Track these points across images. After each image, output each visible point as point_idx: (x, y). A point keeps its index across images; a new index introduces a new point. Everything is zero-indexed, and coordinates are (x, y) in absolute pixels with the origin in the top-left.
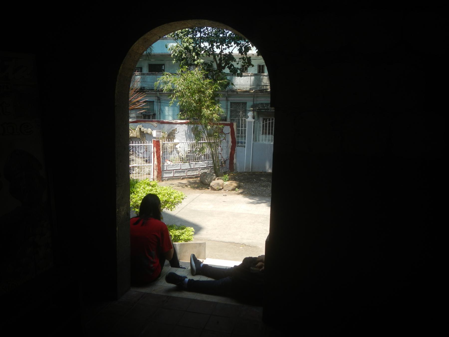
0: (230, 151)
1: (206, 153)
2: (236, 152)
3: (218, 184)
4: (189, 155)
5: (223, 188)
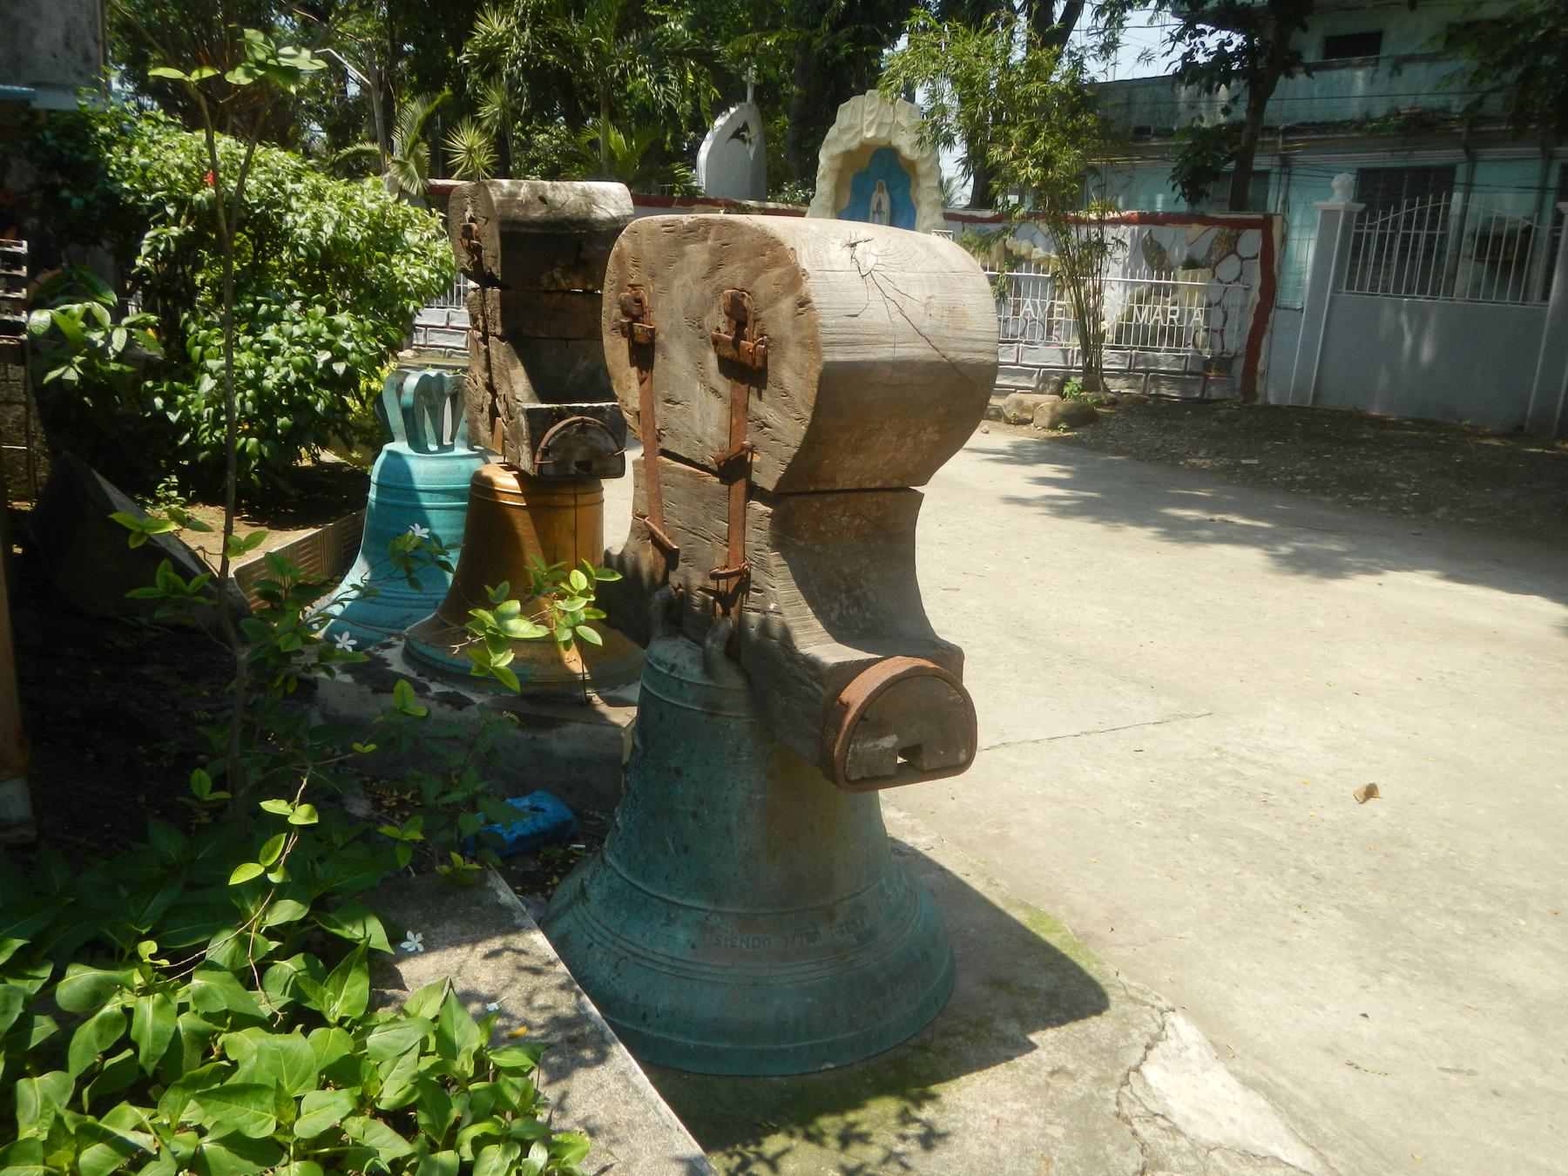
0: (1250, 322)
2: (1272, 331)
3: (1019, 404)
4: (1058, 322)
5: (1032, 421)
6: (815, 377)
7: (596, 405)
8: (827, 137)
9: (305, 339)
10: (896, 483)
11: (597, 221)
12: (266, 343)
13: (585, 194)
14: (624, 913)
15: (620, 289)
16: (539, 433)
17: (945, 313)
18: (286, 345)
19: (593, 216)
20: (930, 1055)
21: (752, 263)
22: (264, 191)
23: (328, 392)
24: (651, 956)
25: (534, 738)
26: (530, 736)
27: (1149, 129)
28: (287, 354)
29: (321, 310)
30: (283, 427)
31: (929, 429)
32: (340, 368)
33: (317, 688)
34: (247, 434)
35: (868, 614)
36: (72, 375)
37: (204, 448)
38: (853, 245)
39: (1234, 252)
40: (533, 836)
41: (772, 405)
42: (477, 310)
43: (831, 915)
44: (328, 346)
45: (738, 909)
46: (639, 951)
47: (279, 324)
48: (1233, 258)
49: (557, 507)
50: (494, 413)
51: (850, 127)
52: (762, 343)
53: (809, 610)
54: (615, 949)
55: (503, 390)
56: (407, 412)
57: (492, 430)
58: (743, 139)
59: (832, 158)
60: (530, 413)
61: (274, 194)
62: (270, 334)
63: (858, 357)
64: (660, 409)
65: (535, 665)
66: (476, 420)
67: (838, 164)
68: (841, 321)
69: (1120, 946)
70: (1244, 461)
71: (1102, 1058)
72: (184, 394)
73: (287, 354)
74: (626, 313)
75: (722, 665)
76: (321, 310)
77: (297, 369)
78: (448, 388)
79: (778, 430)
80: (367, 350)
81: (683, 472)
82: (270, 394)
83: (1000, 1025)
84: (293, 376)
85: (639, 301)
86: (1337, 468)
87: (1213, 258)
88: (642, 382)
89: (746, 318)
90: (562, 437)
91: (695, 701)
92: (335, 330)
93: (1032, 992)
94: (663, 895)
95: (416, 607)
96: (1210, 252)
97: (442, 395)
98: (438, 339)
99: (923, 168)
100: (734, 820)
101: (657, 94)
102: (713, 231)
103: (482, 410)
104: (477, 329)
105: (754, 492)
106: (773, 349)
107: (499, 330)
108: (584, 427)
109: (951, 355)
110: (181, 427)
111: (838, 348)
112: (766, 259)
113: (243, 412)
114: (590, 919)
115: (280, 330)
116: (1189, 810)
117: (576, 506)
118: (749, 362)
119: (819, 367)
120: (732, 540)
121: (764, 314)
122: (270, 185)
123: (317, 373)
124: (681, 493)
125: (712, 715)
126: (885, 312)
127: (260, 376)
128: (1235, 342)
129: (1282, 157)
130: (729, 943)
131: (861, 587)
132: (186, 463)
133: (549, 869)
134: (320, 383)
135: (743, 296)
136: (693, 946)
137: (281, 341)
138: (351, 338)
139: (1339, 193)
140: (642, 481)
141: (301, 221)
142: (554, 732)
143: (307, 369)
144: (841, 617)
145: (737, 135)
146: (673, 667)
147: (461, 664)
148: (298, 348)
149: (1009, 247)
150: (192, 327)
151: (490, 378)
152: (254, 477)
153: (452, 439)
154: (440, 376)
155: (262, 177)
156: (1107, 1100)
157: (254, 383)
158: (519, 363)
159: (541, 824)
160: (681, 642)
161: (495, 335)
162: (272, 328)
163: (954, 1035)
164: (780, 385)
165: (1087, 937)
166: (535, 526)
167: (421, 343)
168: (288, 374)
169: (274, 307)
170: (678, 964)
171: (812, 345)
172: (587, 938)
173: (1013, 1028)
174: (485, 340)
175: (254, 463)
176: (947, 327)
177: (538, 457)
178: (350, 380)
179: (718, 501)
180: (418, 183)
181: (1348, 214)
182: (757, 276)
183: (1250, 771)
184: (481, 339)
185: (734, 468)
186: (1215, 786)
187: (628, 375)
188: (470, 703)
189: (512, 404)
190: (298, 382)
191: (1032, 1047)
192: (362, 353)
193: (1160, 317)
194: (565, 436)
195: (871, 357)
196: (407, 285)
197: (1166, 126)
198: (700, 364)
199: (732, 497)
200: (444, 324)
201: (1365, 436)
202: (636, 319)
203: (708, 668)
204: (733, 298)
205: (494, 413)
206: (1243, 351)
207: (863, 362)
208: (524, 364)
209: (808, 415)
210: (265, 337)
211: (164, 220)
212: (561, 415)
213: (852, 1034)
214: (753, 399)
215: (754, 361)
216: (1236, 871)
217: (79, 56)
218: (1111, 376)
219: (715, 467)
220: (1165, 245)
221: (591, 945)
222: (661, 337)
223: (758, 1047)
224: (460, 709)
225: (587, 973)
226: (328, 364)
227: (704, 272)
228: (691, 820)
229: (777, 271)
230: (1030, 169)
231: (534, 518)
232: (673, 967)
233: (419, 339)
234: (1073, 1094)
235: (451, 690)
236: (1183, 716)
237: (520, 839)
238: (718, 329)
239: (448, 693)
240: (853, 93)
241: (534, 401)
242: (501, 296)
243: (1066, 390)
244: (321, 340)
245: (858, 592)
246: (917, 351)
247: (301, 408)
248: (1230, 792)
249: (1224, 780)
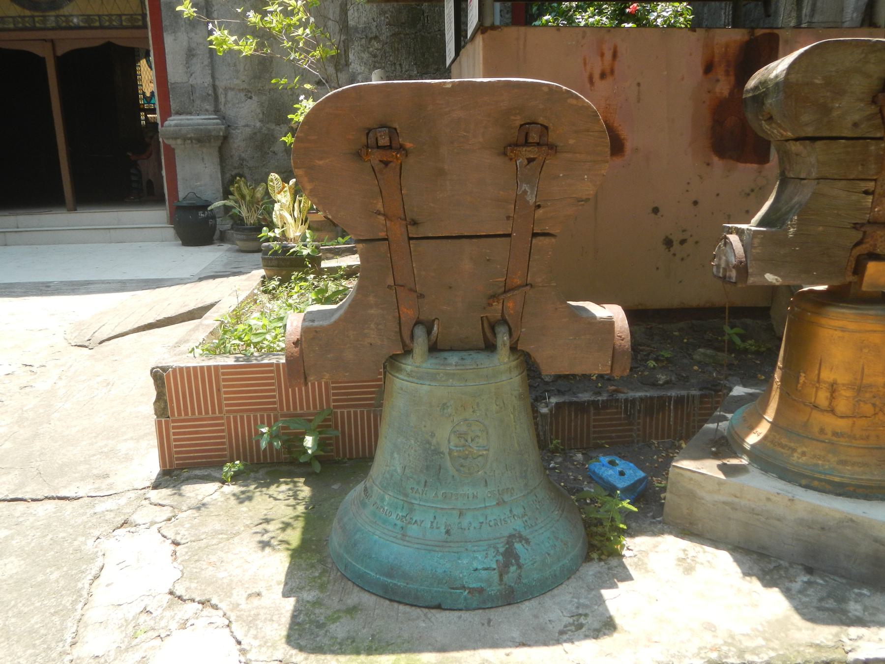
20: (316, 561)
71: (249, 616)
156: (221, 601)
173: (309, 596)
191: (286, 594)
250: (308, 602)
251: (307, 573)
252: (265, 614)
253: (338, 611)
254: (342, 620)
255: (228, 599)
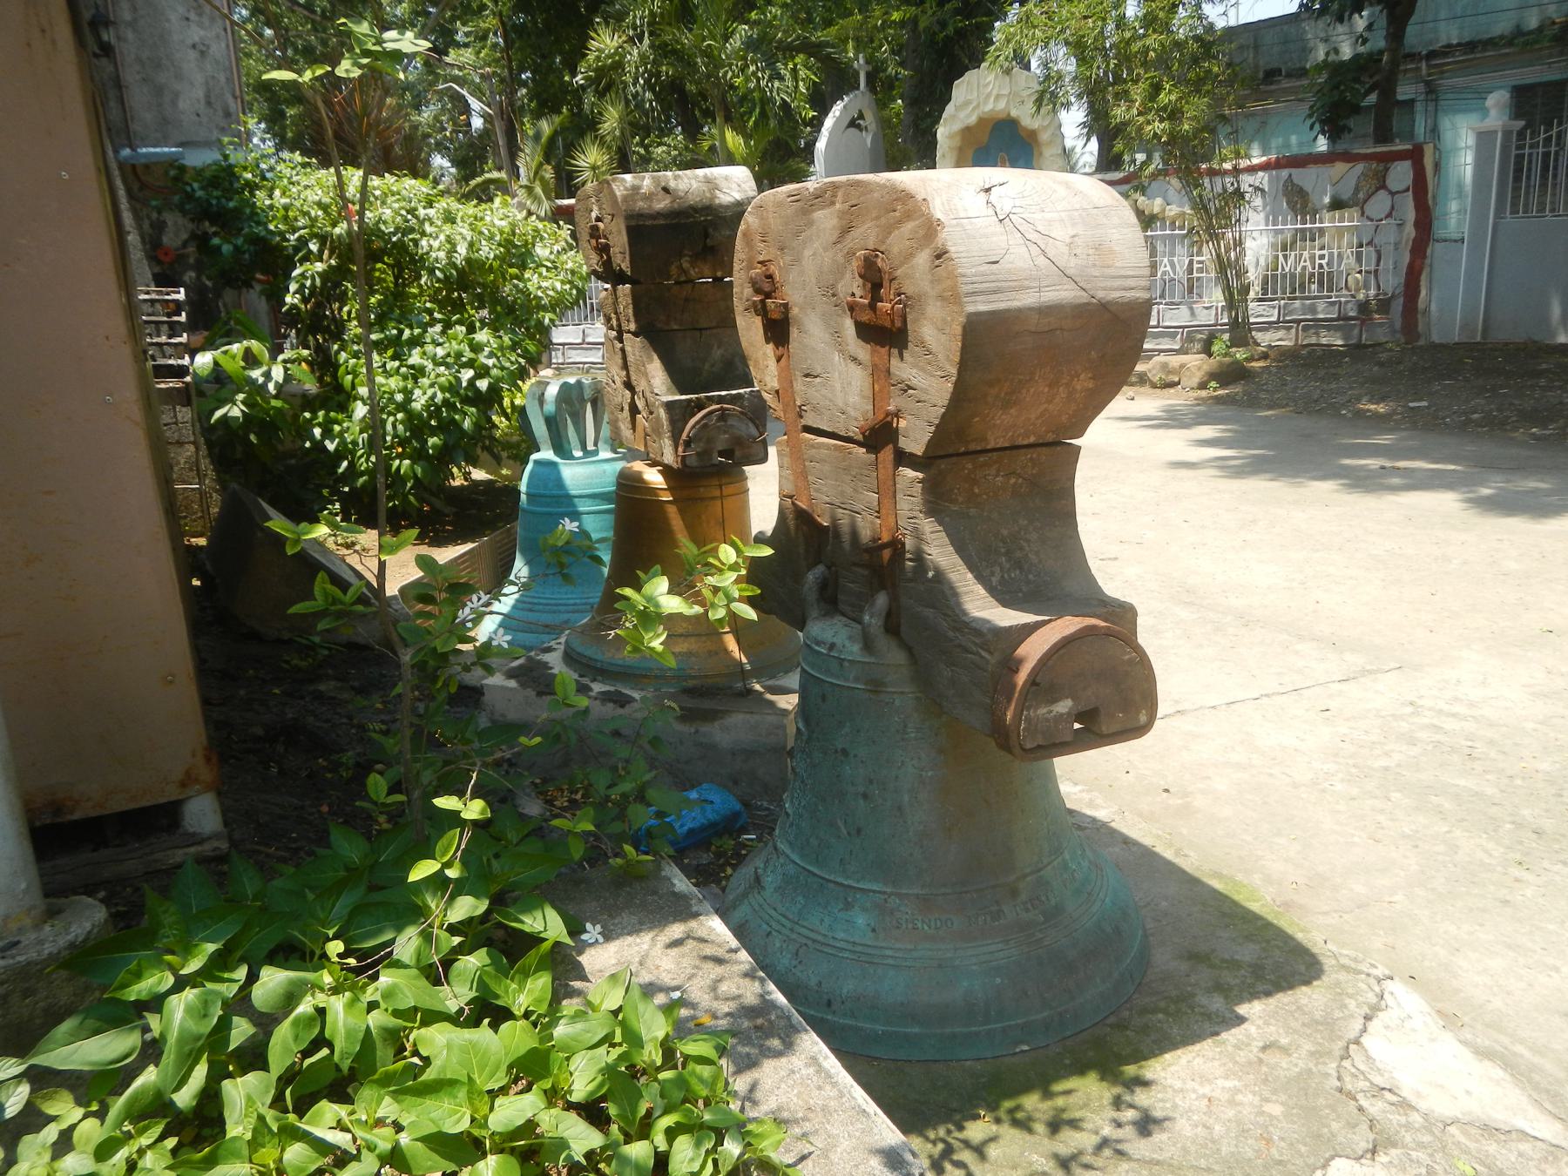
1: (1283, 269)
2: (1431, 266)
3: (1164, 366)
4: (1198, 279)
5: (1179, 383)
6: (958, 330)
7: (734, 392)
8: (944, 116)
9: (448, 360)
10: (1050, 437)
11: (721, 206)
12: (412, 367)
13: (708, 180)
14: (800, 898)
15: (750, 267)
16: (680, 424)
17: (1091, 252)
18: (431, 366)
19: (717, 201)
20: (1128, 1033)
21: (883, 221)
22: (399, 219)
23: (473, 410)
24: (831, 942)
25: (697, 732)
26: (693, 730)
27: (1280, 70)
28: (432, 376)
29: (461, 329)
30: (434, 447)
31: (1082, 377)
32: (483, 384)
33: (483, 694)
34: (401, 457)
35: (1031, 576)
36: (236, 412)
37: (362, 474)
38: (988, 190)
39: (1383, 186)
40: (703, 829)
41: (914, 366)
42: (609, 310)
43: (1014, 893)
44: (470, 364)
45: (916, 891)
46: (819, 938)
47: (422, 347)
48: (1382, 194)
49: (702, 499)
50: (634, 410)
51: (967, 103)
52: (899, 302)
53: (970, 576)
54: (794, 936)
55: (641, 386)
56: (551, 422)
57: (634, 428)
58: (859, 127)
59: (951, 137)
60: (669, 406)
61: (408, 221)
62: (415, 358)
63: (1002, 306)
64: (799, 385)
65: (693, 659)
66: (617, 420)
67: (957, 142)
68: (981, 269)
69: (1326, 913)
70: (1411, 405)
71: (1317, 1031)
72: (339, 424)
73: (432, 376)
74: (758, 291)
75: (884, 643)
76: (461, 329)
77: (443, 389)
78: (588, 394)
79: (925, 391)
80: (508, 365)
81: (828, 447)
82: (420, 415)
83: (1202, 999)
84: (440, 396)
85: (770, 277)
86: (1516, 402)
87: (1361, 195)
88: (778, 360)
89: (881, 278)
90: (703, 426)
91: (857, 680)
92: (476, 348)
93: (1234, 965)
94: (839, 880)
95: (573, 612)
96: (1357, 190)
97: (583, 401)
98: (576, 356)
99: (1044, 137)
100: (906, 798)
101: (771, 91)
102: (840, 194)
103: (622, 410)
104: (611, 328)
105: (902, 458)
106: (912, 307)
107: (633, 327)
108: (723, 416)
109: (1100, 294)
110: (339, 455)
111: (978, 298)
112: (897, 214)
113: (395, 436)
114: (766, 906)
115: (424, 353)
116: (1386, 769)
117: (722, 497)
118: (888, 324)
119: (962, 319)
120: (883, 511)
121: (898, 273)
122: (403, 212)
123: (462, 391)
124: (827, 468)
125: (876, 692)
126: (1027, 255)
127: (409, 399)
128: (1392, 282)
129: (1428, 83)
130: (910, 926)
131: (1021, 549)
132: (346, 489)
133: (722, 861)
134: (466, 401)
135: (877, 256)
136: (874, 930)
137: (426, 363)
138: (490, 356)
139: (1495, 111)
140: (786, 460)
141: (436, 244)
142: (716, 724)
143: (452, 388)
144: (1002, 581)
145: (853, 124)
146: (832, 646)
147: (620, 662)
148: (442, 368)
149: (1141, 208)
150: (343, 356)
151: (628, 375)
152: (411, 498)
153: (596, 444)
154: (579, 382)
155: (396, 205)
156: (1327, 1075)
157: (404, 406)
158: (655, 357)
159: (710, 817)
160: (839, 621)
161: (629, 332)
162: (416, 351)
163: (1155, 1011)
164: (922, 344)
165: (1287, 905)
166: (683, 520)
167: (560, 361)
168: (434, 396)
169: (417, 331)
170: (859, 949)
171: (952, 297)
172: (765, 926)
173: (1217, 1003)
174: (620, 339)
175: (409, 485)
176: (1094, 265)
177: (680, 449)
178: (494, 393)
179: (866, 472)
180: (546, 205)
181: (1507, 134)
182: (890, 233)
183: (1450, 724)
184: (616, 338)
185: (880, 436)
186: (1413, 742)
187: (764, 354)
188: (630, 700)
189: (651, 399)
190: (446, 402)
191: (1241, 1020)
192: (502, 368)
193: (1308, 263)
194: (705, 426)
195: (1016, 304)
196: (541, 298)
197: (1298, 65)
198: (837, 333)
199: (880, 466)
200: (579, 341)
201: (1544, 366)
202: (768, 295)
203: (868, 645)
204: (866, 259)
205: (634, 410)
206: (1401, 289)
207: (1007, 311)
208: (660, 358)
209: (954, 371)
210: (411, 361)
211: (307, 258)
212: (700, 405)
213: (1046, 1014)
214: (895, 362)
215: (893, 321)
216: (1446, 829)
217: (220, 113)
218: (1259, 330)
219: (860, 437)
220: (1308, 187)
221: (769, 934)
222: (795, 311)
223: (948, 1030)
224: (622, 706)
225: (768, 961)
226: (471, 382)
227: (834, 238)
228: (862, 802)
229: (910, 225)
230: (1157, 123)
231: (682, 511)
232: (855, 952)
233: (557, 357)
234: (1288, 1069)
235: (612, 689)
236: (1370, 672)
237: (691, 832)
238: (853, 295)
239: (608, 692)
240: (967, 69)
241: (673, 394)
242: (633, 291)
243: (1215, 348)
244: (464, 359)
245: (1018, 554)
246: (1065, 293)
247: (448, 427)
248: (1430, 747)
249: (1423, 735)
250: (1226, 997)
251: (1165, 1026)
252: (1297, 1020)
253: (1212, 966)
254: (1227, 957)
255: (1314, 1069)
